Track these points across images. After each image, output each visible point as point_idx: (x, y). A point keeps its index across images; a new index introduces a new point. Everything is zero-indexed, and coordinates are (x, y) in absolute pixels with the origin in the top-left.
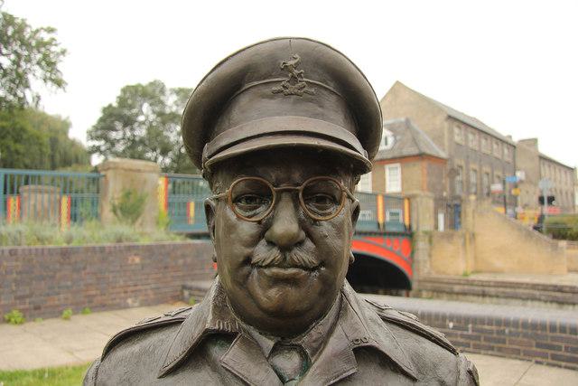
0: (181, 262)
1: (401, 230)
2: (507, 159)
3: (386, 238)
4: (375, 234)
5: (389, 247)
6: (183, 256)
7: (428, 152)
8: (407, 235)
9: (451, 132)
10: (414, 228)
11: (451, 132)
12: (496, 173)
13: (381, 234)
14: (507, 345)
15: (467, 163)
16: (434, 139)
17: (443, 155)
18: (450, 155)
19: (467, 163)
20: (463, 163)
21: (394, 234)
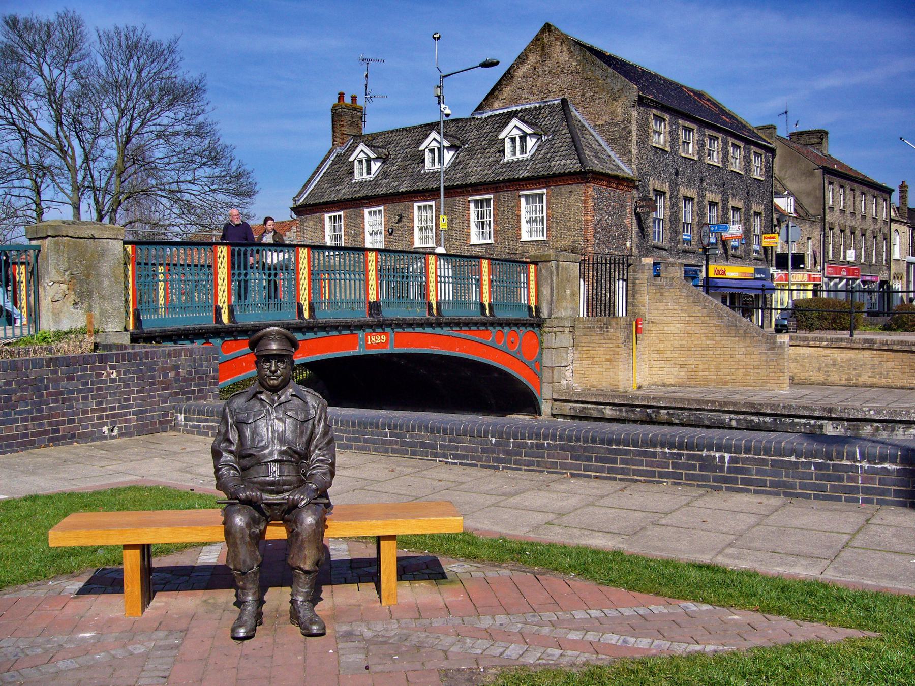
0: (172, 375)
1: (523, 315)
2: (757, 175)
3: (493, 331)
4: (476, 324)
5: (501, 345)
6: (176, 368)
7: (598, 167)
8: (532, 325)
9: (644, 127)
10: (545, 313)
11: (644, 127)
12: (732, 203)
13: (484, 324)
14: (547, 459)
15: (674, 186)
16: (611, 141)
17: (628, 171)
18: (640, 170)
19: (674, 186)
20: (666, 188)
21: (509, 323)
